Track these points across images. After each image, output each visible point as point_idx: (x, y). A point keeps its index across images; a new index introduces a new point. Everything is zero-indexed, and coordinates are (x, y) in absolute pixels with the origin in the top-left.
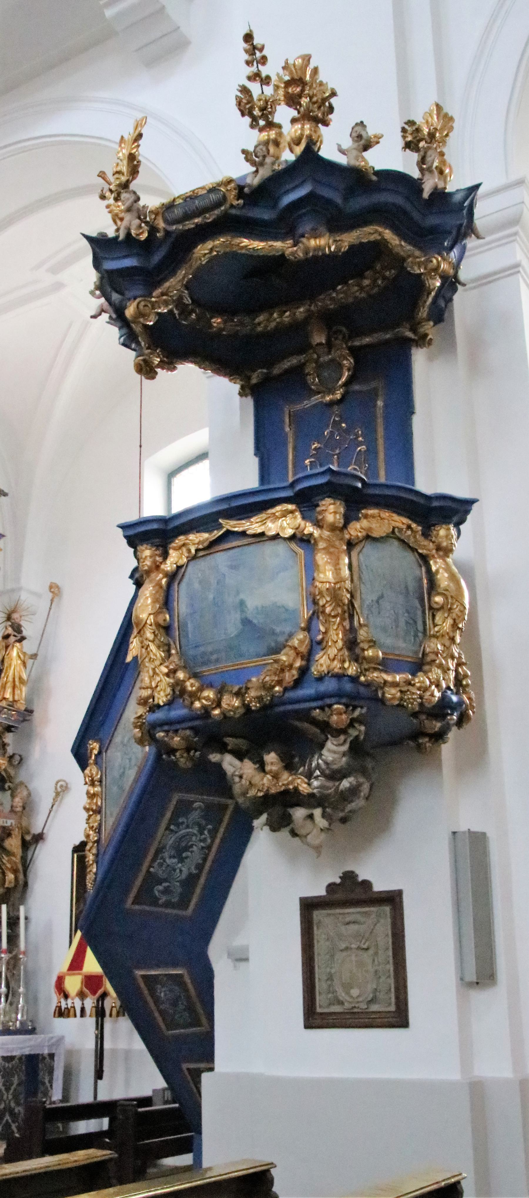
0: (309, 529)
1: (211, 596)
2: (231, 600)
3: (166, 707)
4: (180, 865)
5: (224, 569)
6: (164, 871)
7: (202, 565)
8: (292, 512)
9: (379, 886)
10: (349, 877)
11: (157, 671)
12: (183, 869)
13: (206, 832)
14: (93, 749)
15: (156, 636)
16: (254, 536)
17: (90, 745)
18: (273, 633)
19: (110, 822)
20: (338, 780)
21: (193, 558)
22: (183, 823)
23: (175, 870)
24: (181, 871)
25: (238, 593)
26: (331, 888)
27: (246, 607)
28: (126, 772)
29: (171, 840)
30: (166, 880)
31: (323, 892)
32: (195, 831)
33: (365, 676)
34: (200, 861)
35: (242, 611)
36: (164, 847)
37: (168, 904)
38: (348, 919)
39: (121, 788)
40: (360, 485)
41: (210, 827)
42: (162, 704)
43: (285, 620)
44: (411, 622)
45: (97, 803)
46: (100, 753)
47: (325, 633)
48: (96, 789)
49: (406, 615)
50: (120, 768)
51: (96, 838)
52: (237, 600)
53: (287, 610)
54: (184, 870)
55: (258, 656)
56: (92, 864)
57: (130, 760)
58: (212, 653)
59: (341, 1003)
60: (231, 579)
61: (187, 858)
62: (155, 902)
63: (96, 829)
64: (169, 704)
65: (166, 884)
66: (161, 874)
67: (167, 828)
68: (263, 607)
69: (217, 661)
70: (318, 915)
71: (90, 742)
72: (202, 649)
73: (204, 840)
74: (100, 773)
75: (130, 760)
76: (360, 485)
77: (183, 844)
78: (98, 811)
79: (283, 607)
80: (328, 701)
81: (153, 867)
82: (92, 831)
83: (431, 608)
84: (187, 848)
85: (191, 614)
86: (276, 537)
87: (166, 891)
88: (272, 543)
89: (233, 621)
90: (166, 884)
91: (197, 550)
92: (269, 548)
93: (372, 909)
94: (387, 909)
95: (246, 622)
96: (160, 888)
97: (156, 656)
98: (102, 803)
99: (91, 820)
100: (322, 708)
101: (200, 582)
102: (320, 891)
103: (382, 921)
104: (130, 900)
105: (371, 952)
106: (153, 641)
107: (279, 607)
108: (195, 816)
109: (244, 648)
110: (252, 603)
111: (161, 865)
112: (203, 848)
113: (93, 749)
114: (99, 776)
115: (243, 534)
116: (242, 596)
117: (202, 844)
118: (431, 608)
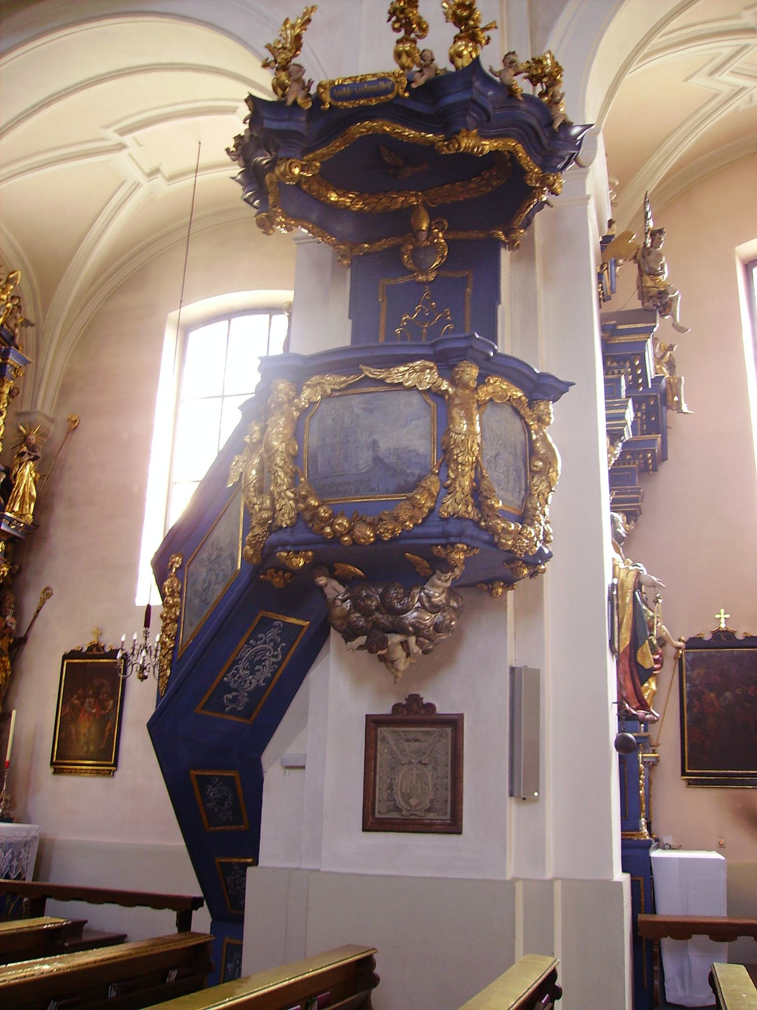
0: (445, 386)
3: (289, 529)
4: (251, 677)
5: (357, 411)
6: (235, 681)
8: (431, 368)
9: (442, 708)
10: (414, 699)
11: (283, 494)
12: (253, 681)
13: (279, 649)
14: (174, 563)
15: (285, 463)
16: (392, 385)
17: (173, 558)
19: (190, 631)
20: (434, 614)
22: (261, 639)
23: (245, 682)
24: (250, 683)
26: (396, 707)
28: (212, 587)
29: (247, 654)
30: (236, 690)
32: (270, 646)
33: (485, 521)
34: (270, 676)
36: (241, 659)
37: (234, 712)
38: (411, 736)
39: (205, 601)
40: (492, 354)
41: (284, 644)
42: (285, 526)
44: (518, 479)
45: (175, 613)
46: (181, 566)
47: (455, 479)
48: (175, 600)
49: (514, 473)
51: (172, 645)
53: (418, 455)
54: (254, 681)
55: (387, 492)
56: (166, 669)
57: (217, 576)
59: (398, 809)
61: (258, 671)
62: (221, 708)
63: (172, 637)
64: (291, 527)
65: (235, 694)
66: (233, 685)
67: (247, 642)
71: (173, 556)
73: (275, 656)
74: (180, 586)
75: (217, 576)
76: (492, 354)
77: (257, 658)
78: (177, 620)
79: (414, 451)
80: (452, 539)
81: (227, 677)
82: (169, 638)
83: (531, 470)
84: (260, 662)
86: (413, 388)
87: (234, 700)
88: (407, 393)
90: (235, 694)
91: (333, 390)
92: (404, 397)
93: (434, 729)
94: (449, 730)
96: (230, 696)
97: (284, 481)
98: (180, 613)
99: (168, 628)
100: (444, 546)
102: (385, 709)
103: (443, 740)
104: (200, 705)
105: (430, 767)
106: (281, 468)
107: (410, 451)
108: (272, 633)
110: (385, 445)
111: (234, 675)
112: (273, 663)
113: (174, 563)
114: (179, 588)
115: (382, 382)
116: (375, 437)
117: (274, 660)
118: (531, 470)
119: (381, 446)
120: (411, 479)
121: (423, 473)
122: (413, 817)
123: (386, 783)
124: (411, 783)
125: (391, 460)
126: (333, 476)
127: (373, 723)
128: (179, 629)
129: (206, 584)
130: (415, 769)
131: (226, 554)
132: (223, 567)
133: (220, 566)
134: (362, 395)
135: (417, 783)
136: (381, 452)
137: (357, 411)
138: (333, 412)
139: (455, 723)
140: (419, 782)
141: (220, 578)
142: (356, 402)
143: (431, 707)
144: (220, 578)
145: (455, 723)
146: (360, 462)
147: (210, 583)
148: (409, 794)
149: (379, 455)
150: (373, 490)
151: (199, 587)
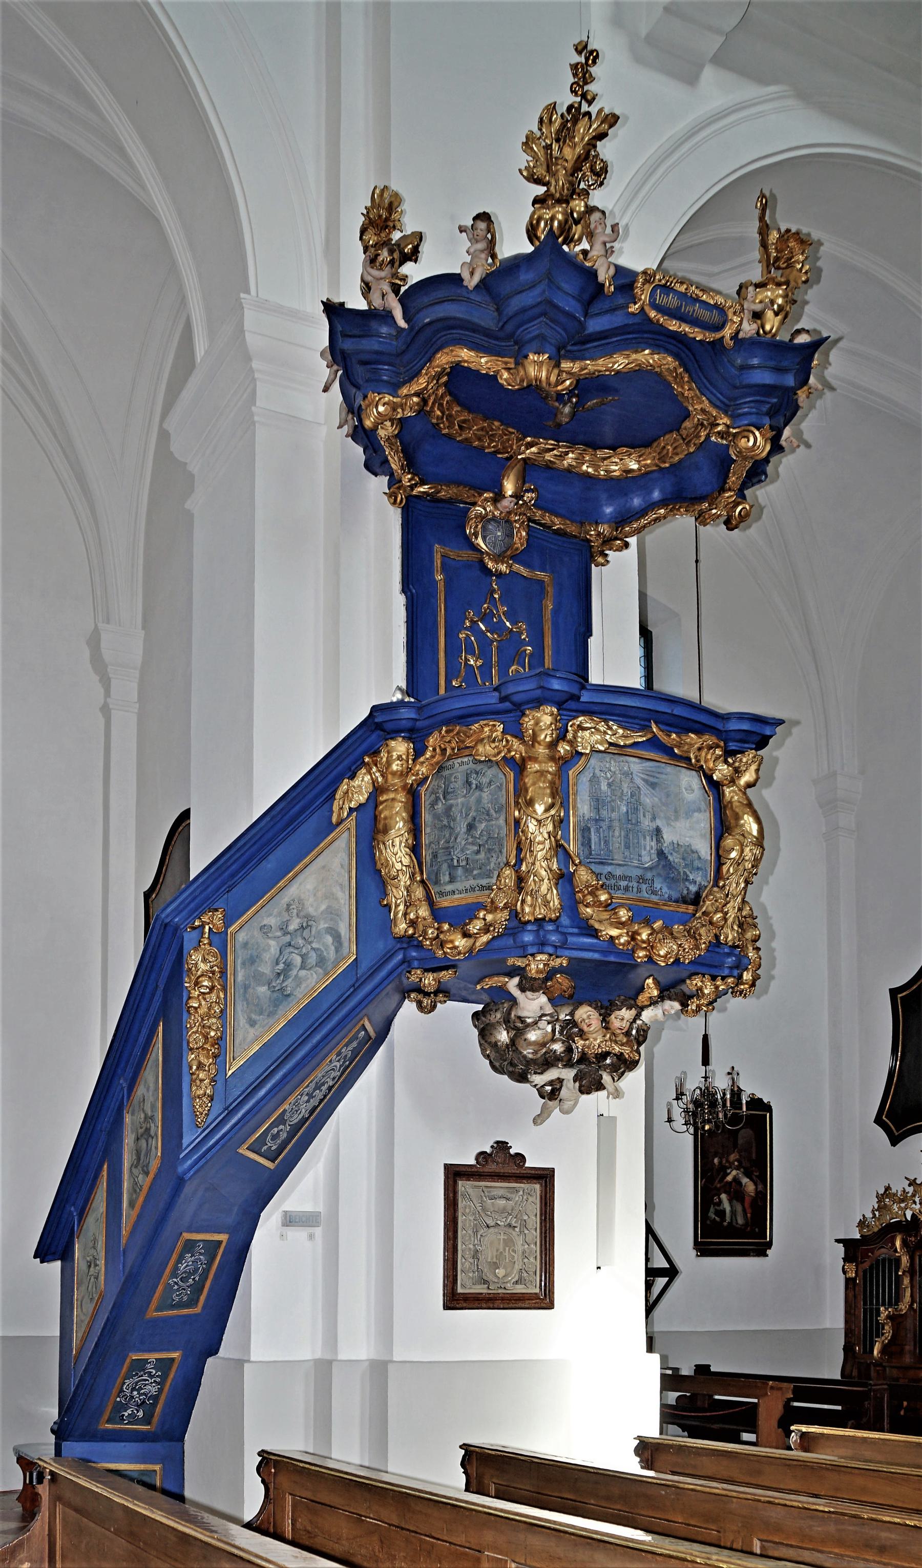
1: (624, 809)
2: (647, 823)
7: (614, 764)
25: (654, 818)
27: (662, 837)
31: (472, 1162)
35: (658, 841)
39: (283, 996)
50: (277, 964)
58: (625, 878)
69: (627, 889)
70: (464, 1186)
75: (304, 957)
85: (596, 821)
95: (661, 854)
101: (609, 785)
102: (470, 1160)
109: (657, 885)
110: (668, 836)
116: (659, 823)
119: (665, 837)
122: (500, 1291)
123: (470, 1249)
124: (497, 1251)
126: (612, 864)
127: (454, 1174)
128: (224, 1026)
129: (281, 966)
130: (502, 1234)
131: (323, 925)
132: (314, 945)
133: (310, 943)
135: (505, 1250)
136: (665, 845)
138: (609, 776)
139: (545, 1177)
140: (507, 1249)
141: (313, 959)
143: (521, 1157)
144: (313, 959)
145: (545, 1177)
146: (643, 853)
147: (288, 965)
148: (495, 1263)
151: (266, 969)
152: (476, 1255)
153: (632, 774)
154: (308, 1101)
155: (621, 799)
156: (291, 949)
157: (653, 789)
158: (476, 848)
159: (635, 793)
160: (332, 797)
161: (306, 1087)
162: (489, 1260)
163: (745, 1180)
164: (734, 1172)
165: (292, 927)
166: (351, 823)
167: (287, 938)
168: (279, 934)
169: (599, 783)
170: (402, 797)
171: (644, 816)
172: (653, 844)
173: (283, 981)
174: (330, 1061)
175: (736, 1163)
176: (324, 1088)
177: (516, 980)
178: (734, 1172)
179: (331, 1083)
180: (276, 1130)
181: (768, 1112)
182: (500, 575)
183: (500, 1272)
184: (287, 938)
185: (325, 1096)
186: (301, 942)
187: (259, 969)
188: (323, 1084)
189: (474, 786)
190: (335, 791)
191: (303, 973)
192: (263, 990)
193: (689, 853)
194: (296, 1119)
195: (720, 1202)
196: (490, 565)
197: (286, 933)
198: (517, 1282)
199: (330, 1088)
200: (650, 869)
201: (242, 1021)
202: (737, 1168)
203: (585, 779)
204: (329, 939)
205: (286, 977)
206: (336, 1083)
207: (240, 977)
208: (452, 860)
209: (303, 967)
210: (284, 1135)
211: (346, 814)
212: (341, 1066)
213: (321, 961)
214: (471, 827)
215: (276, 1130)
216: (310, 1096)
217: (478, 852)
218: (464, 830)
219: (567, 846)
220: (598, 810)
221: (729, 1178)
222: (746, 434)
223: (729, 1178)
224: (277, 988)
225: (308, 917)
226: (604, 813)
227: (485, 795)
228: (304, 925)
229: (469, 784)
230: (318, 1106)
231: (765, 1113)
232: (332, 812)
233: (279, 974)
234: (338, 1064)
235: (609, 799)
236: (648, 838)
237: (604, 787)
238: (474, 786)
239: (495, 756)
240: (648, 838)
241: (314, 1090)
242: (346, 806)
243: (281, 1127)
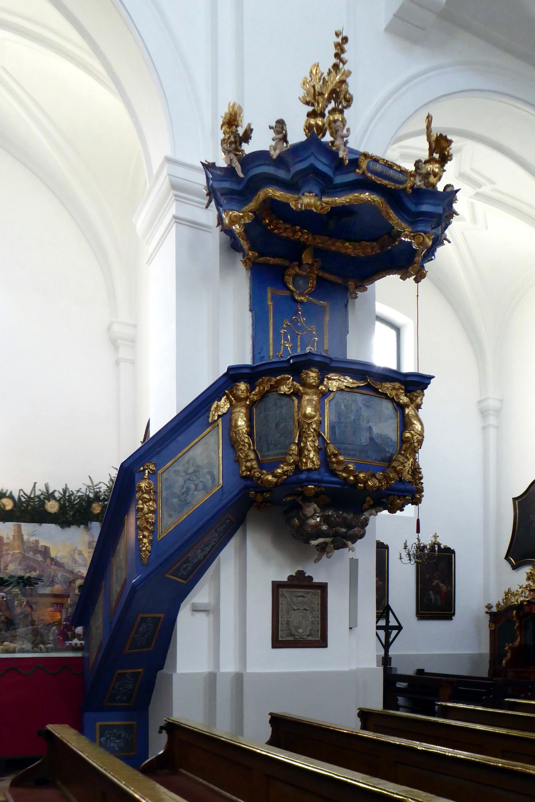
1: (353, 418)
2: (364, 424)
5: (360, 405)
18: (385, 451)
21: (340, 390)
25: (368, 422)
28: (191, 492)
39: (186, 503)
43: (391, 446)
50: (183, 487)
52: (368, 425)
53: (391, 440)
57: (196, 485)
60: (365, 413)
68: (380, 434)
72: (345, 446)
75: (196, 485)
79: (390, 438)
80: (406, 494)
89: (365, 436)
95: (372, 439)
101: (345, 406)
107: (388, 438)
110: (375, 430)
116: (371, 424)
119: (374, 431)
120: (388, 455)
121: (393, 453)
125: (379, 441)
129: (185, 489)
131: (205, 471)
132: (201, 480)
134: (362, 394)
136: (374, 434)
137: (360, 405)
138: (345, 401)
141: (201, 486)
142: (359, 398)
144: (201, 486)
146: (363, 438)
147: (188, 489)
149: (373, 436)
150: (368, 457)
151: (177, 491)
152: (288, 623)
153: (357, 401)
154: (201, 552)
155: (351, 412)
156: (190, 482)
157: (368, 408)
158: (279, 435)
159: (358, 410)
160: (209, 410)
161: (200, 546)
162: (295, 625)
163: (442, 585)
164: (436, 581)
165: (191, 470)
166: (220, 422)
167: (188, 476)
168: (183, 474)
169: (340, 405)
170: (243, 410)
171: (363, 421)
172: (368, 434)
173: (186, 497)
174: (212, 534)
175: (437, 577)
176: (210, 546)
177: (301, 498)
178: (436, 581)
179: (213, 544)
180: (185, 566)
181: (453, 554)
182: (301, 302)
183: (300, 631)
184: (188, 476)
185: (211, 550)
186: (195, 478)
187: (174, 491)
188: (209, 544)
189: (279, 406)
190: (211, 407)
191: (196, 493)
192: (175, 500)
193: (386, 439)
194: (196, 561)
195: (429, 595)
196: (296, 298)
197: (187, 474)
198: (308, 636)
199: (213, 546)
200: (366, 445)
201: (165, 515)
202: (438, 579)
203: (333, 403)
204: (209, 477)
205: (187, 495)
206: (217, 544)
207: (164, 495)
208: (268, 441)
209: (196, 490)
210: (190, 568)
211: (216, 418)
212: (218, 536)
213: (205, 488)
214: (277, 425)
215: (185, 566)
216: (203, 550)
217: (280, 437)
218: (274, 425)
219: (324, 435)
220: (339, 418)
221: (434, 584)
222: (418, 236)
223: (434, 584)
224: (183, 500)
225: (199, 466)
226: (343, 420)
227: (284, 410)
228: (196, 470)
229: (276, 405)
230: (208, 554)
231: (452, 554)
232: (208, 417)
233: (183, 493)
234: (217, 535)
235: (345, 413)
236: (365, 431)
237: (343, 407)
238: (279, 406)
239: (288, 391)
240: (365, 431)
241: (205, 547)
242: (216, 414)
243: (188, 564)
